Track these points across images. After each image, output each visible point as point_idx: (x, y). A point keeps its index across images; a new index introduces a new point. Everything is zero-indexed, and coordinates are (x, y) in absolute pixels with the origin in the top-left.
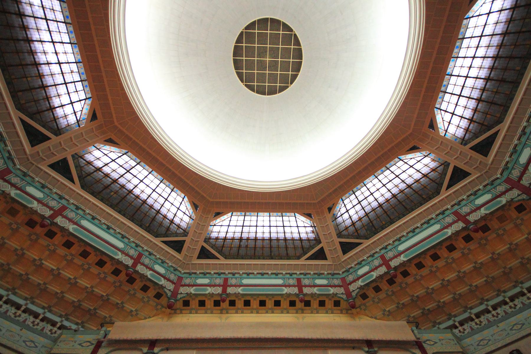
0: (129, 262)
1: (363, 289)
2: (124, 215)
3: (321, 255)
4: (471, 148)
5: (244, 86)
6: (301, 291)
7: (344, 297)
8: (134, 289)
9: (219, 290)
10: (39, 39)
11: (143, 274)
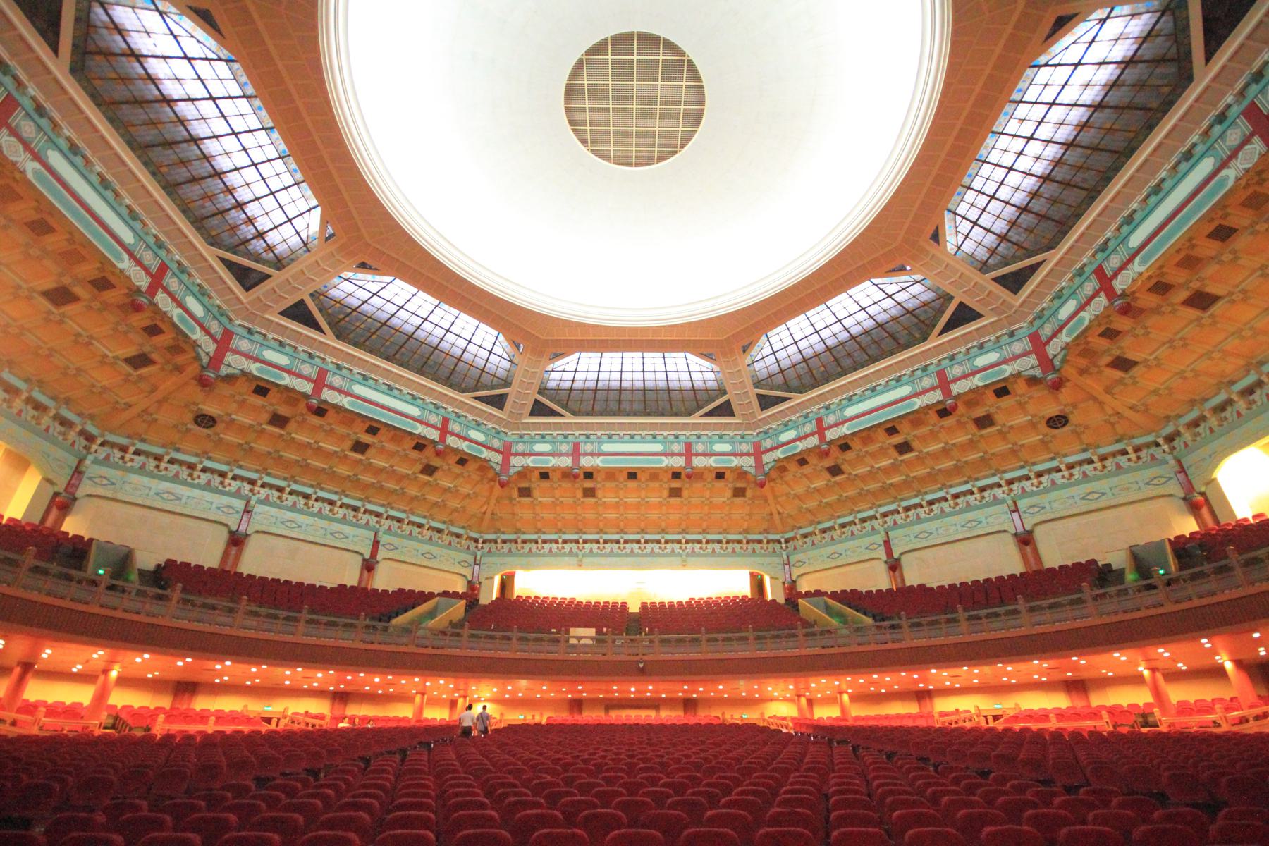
3: (726, 410)
4: (995, 280)
6: (689, 461)
10: (211, 135)
11: (457, 449)
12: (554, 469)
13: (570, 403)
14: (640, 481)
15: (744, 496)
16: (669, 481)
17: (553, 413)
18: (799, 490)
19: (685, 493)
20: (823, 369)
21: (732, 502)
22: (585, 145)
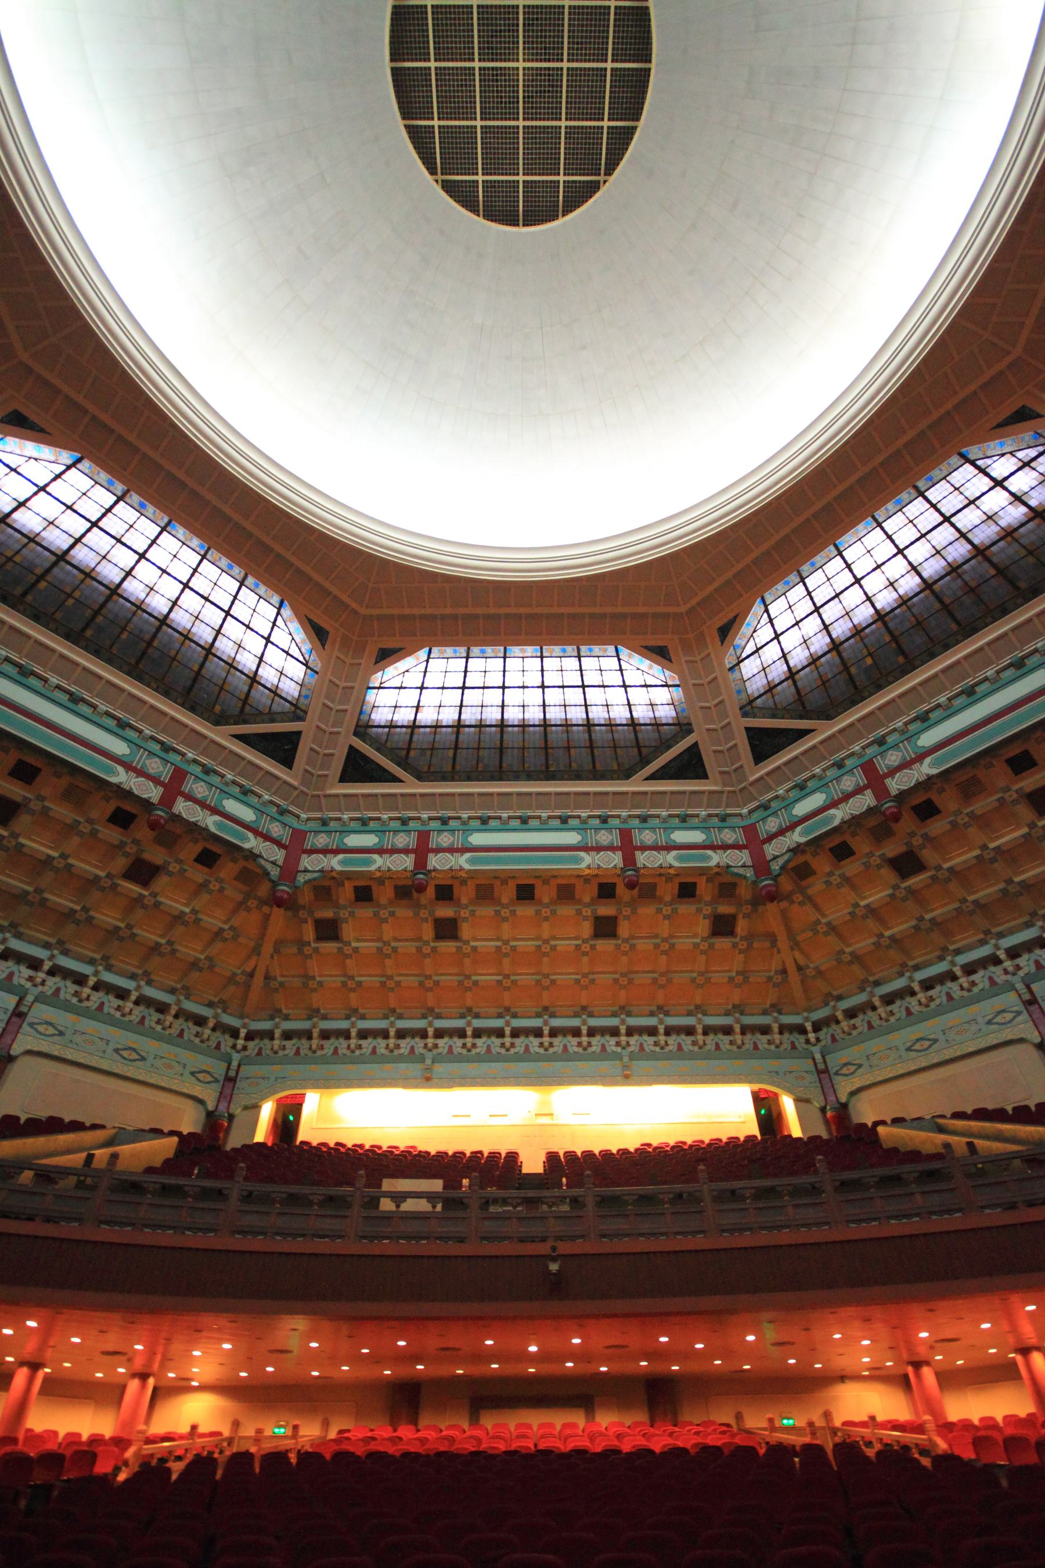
0: (153, 793)
1: (804, 852)
2: (110, 661)
5: (438, 189)
6: (629, 860)
7: (749, 873)
8: (180, 862)
9: (407, 862)
11: (195, 824)
12: (383, 878)
13: (412, 753)
14: (540, 902)
15: (732, 933)
16: (593, 902)
17: (384, 776)
18: (837, 913)
19: (624, 929)
20: (869, 661)
21: (711, 946)
22: (432, 171)
